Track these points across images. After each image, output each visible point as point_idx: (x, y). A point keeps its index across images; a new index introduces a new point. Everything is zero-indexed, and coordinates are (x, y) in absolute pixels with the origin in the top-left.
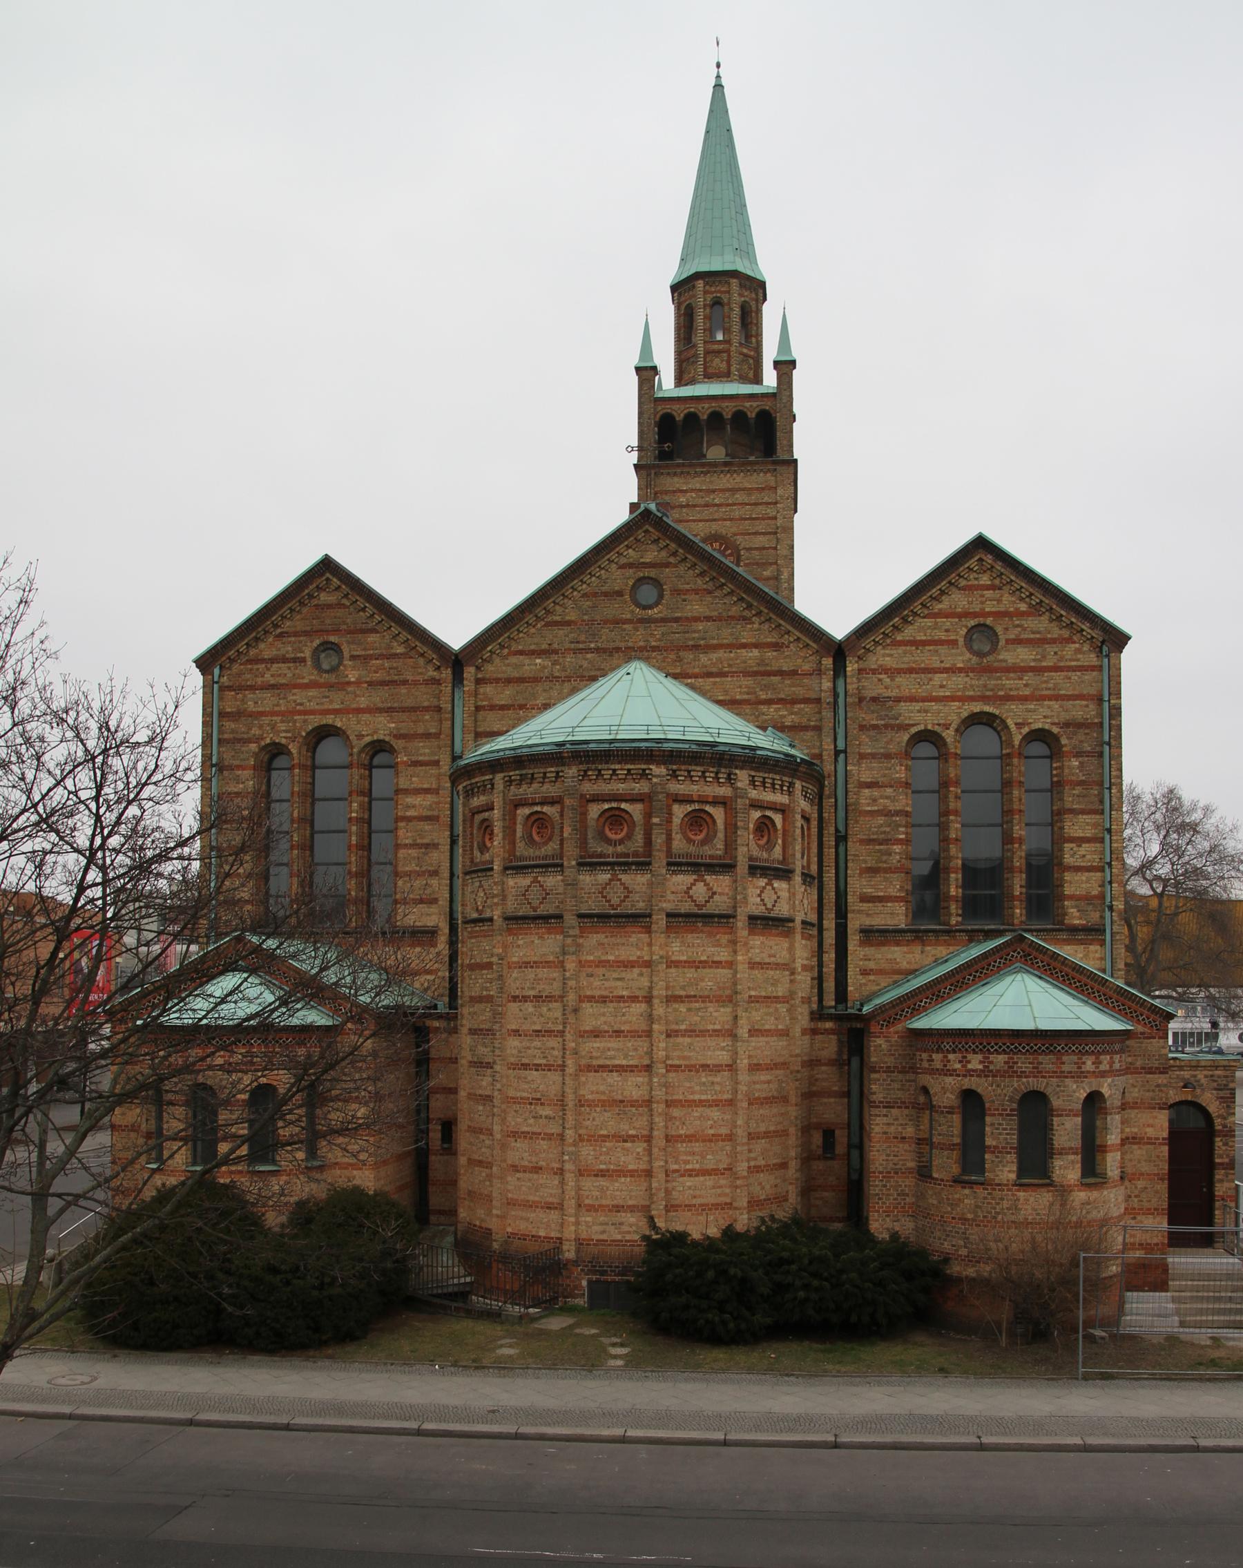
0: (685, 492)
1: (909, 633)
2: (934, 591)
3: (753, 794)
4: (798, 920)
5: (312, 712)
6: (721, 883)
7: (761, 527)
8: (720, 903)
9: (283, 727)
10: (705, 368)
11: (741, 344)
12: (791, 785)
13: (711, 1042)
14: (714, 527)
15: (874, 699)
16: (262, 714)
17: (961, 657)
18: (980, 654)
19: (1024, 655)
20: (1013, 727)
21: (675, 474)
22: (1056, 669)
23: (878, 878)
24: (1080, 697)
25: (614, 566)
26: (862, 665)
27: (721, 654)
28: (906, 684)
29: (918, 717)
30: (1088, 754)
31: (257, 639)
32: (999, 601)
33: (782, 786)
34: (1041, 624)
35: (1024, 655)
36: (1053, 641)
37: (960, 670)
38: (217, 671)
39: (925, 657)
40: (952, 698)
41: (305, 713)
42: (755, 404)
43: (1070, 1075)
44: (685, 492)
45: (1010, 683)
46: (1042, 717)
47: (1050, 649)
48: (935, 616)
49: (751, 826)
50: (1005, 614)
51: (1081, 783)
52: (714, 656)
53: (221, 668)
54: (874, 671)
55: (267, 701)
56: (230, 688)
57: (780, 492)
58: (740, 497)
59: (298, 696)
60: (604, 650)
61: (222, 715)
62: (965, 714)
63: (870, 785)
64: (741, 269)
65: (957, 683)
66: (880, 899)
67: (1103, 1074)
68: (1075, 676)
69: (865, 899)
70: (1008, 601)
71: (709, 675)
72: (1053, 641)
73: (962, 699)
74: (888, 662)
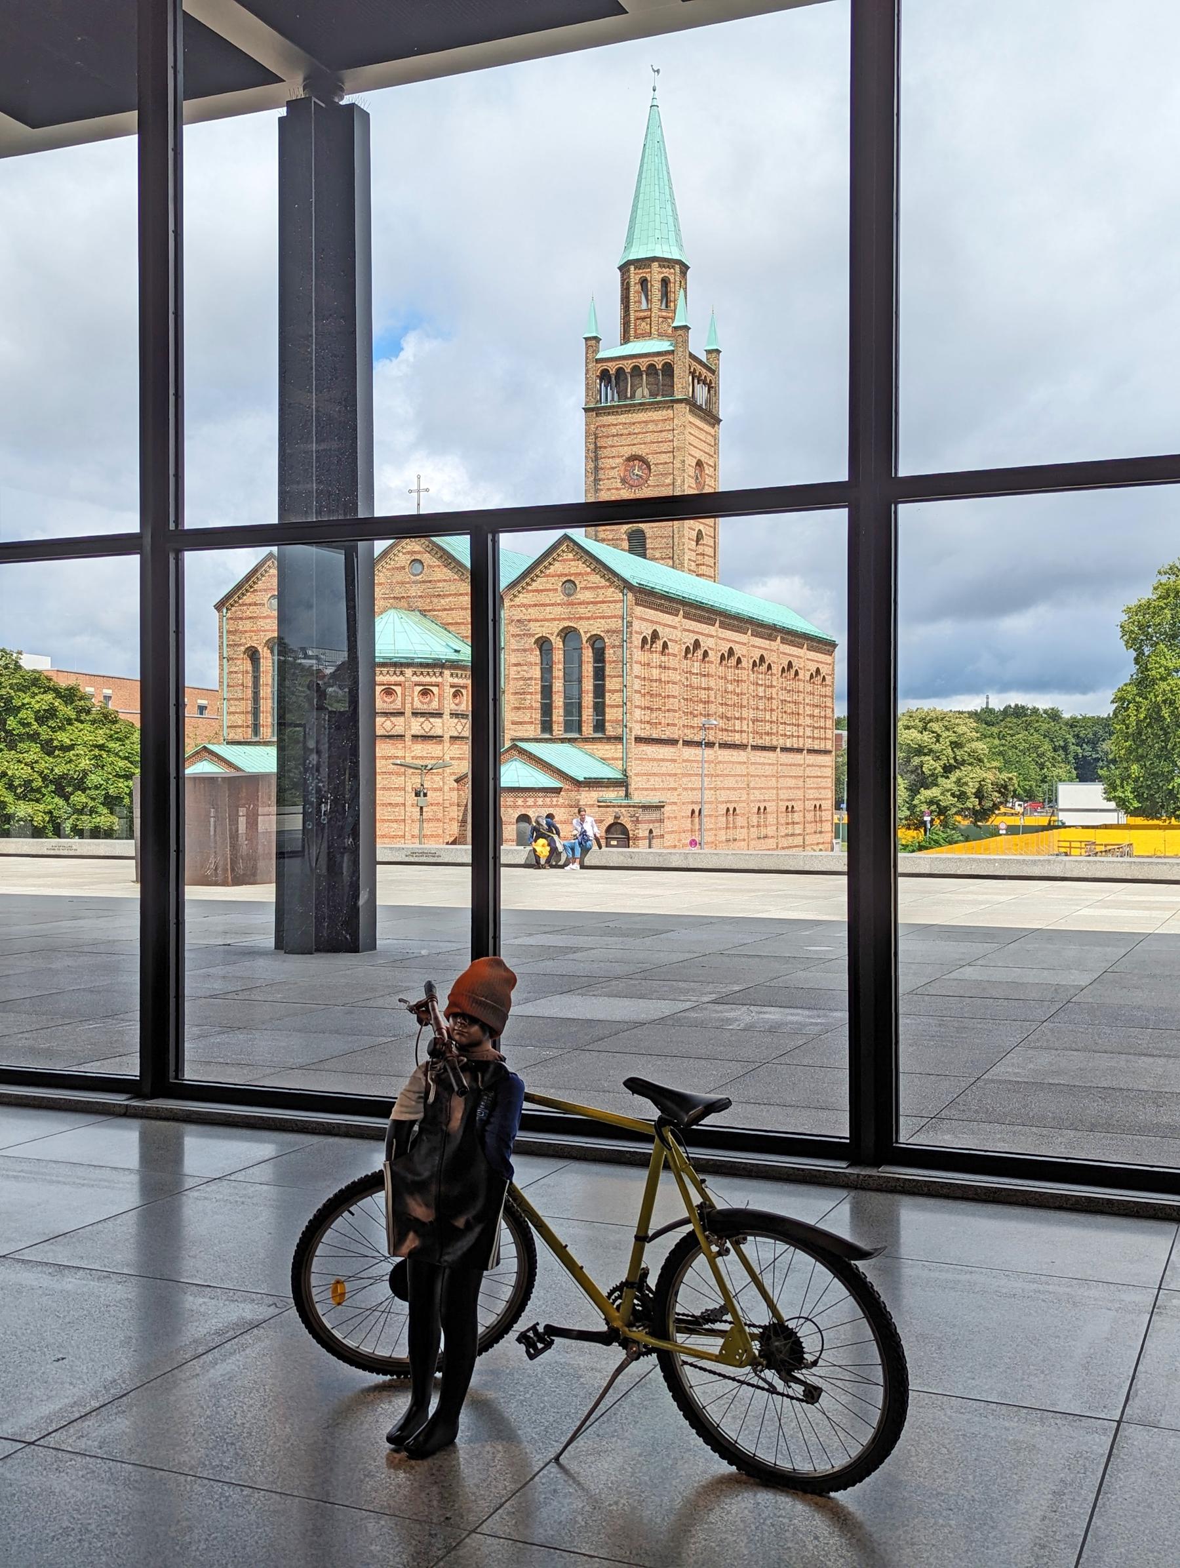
0: (616, 425)
1: (534, 585)
2: (546, 563)
3: (415, 679)
4: (447, 737)
5: (268, 631)
6: (400, 720)
7: (665, 447)
8: (398, 730)
9: (255, 638)
10: (635, 332)
11: (660, 310)
12: (441, 673)
13: (393, 793)
14: (635, 450)
15: (518, 621)
16: (246, 631)
17: (560, 597)
18: (569, 595)
19: (587, 596)
20: (582, 634)
21: (609, 413)
22: (603, 602)
23: (520, 712)
24: (615, 617)
25: (401, 554)
26: (512, 603)
27: (450, 598)
28: (533, 613)
29: (538, 630)
30: (618, 647)
31: (243, 595)
32: (577, 567)
33: (435, 674)
34: (596, 579)
35: (587, 596)
36: (603, 587)
37: (559, 604)
38: (225, 610)
39: (543, 598)
40: (554, 619)
41: (265, 631)
42: (661, 358)
43: (510, 806)
44: (616, 425)
45: (582, 610)
46: (597, 628)
47: (601, 591)
48: (548, 576)
49: (416, 693)
50: (580, 574)
51: (614, 662)
52: (447, 600)
53: (227, 609)
54: (519, 606)
55: (248, 625)
56: (231, 618)
57: (676, 421)
58: (651, 427)
59: (261, 622)
60: (397, 598)
61: (229, 632)
62: (561, 628)
63: (516, 665)
64: (658, 254)
65: (559, 609)
66: (521, 723)
67: (529, 807)
68: (612, 606)
69: (513, 723)
70: (581, 567)
71: (445, 610)
72: (603, 587)
73: (559, 620)
74: (525, 601)
